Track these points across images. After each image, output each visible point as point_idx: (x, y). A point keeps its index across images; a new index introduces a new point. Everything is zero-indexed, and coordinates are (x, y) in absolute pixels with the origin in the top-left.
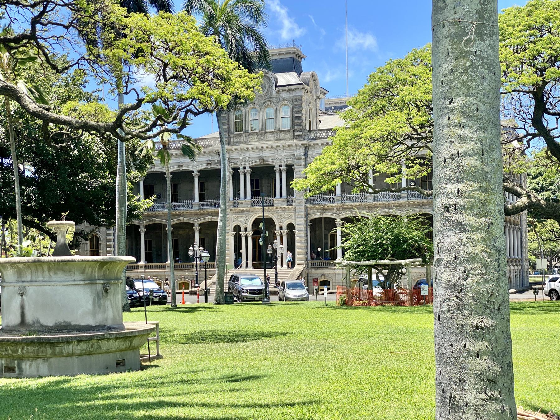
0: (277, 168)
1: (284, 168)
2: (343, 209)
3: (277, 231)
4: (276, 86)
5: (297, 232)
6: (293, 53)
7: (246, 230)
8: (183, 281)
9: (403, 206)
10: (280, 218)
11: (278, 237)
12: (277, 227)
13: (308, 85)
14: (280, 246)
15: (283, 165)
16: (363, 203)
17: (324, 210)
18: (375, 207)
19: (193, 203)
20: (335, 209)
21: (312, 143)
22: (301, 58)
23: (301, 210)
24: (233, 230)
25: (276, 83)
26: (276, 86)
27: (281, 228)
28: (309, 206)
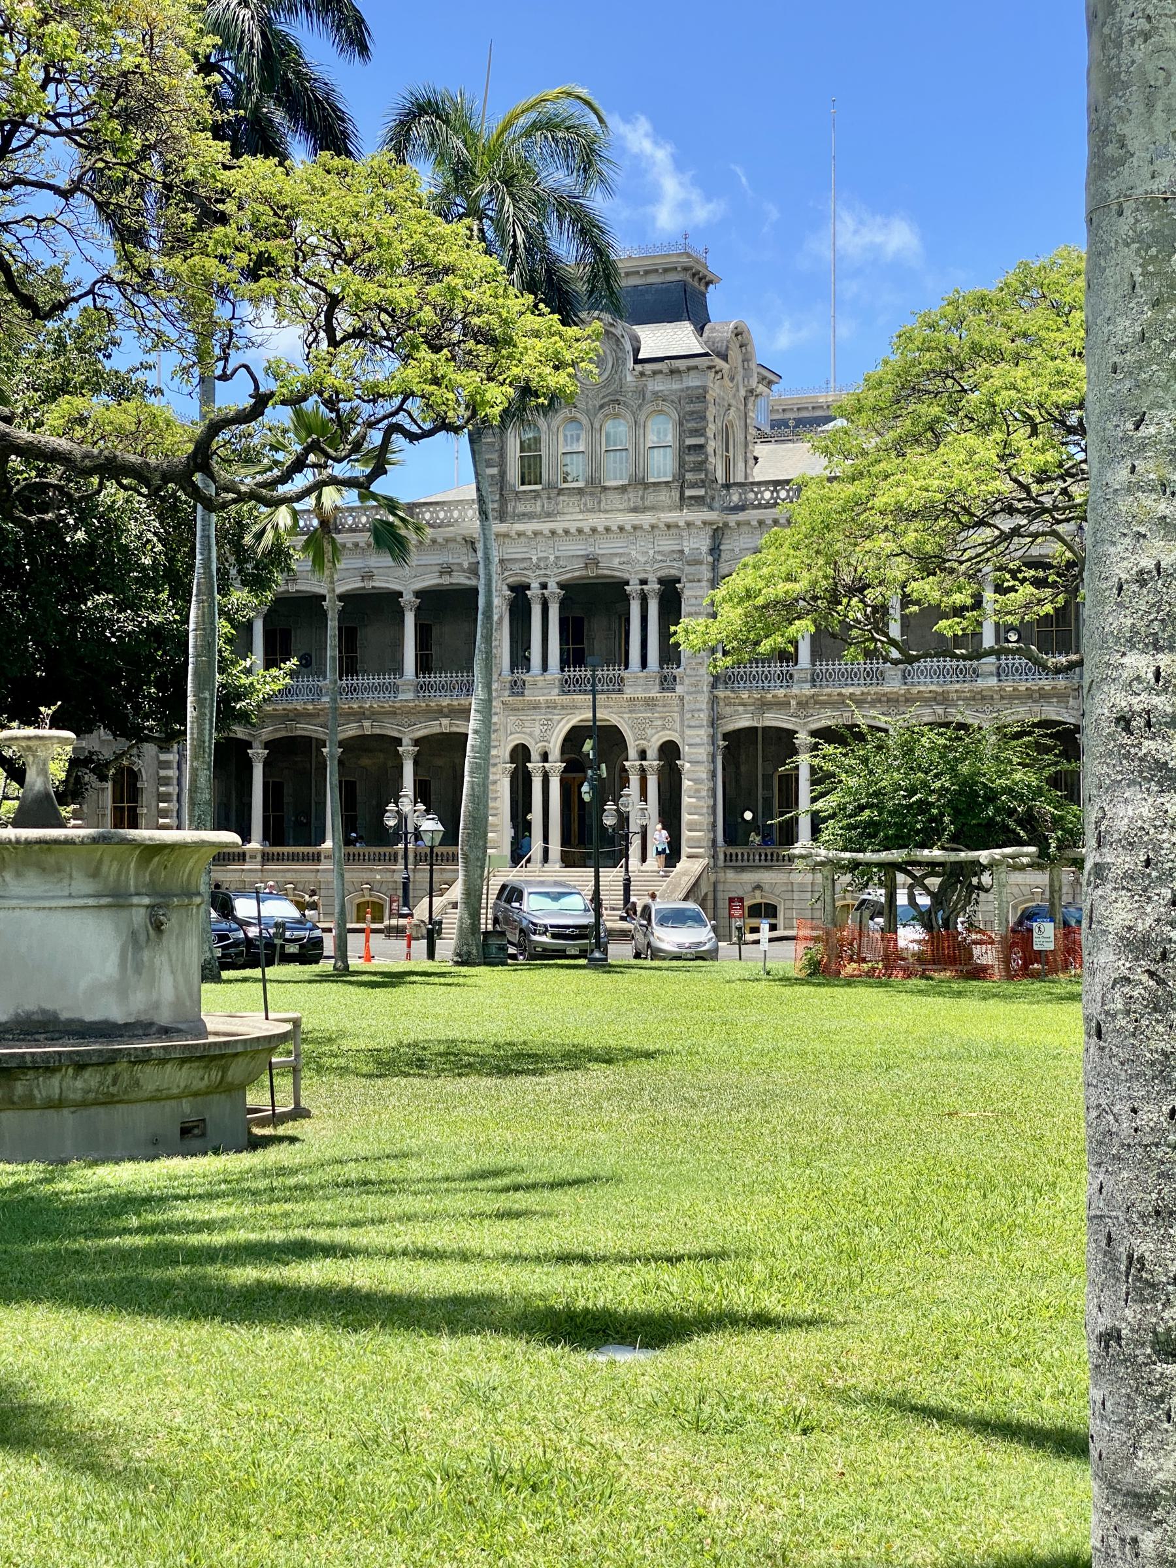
0: (633, 588)
1: (653, 586)
2: (816, 703)
3: (633, 763)
4: (637, 361)
5: (687, 765)
6: (686, 269)
7: (545, 757)
8: (367, 898)
9: (983, 698)
10: (641, 727)
11: (634, 780)
12: (632, 753)
13: (724, 357)
14: (639, 807)
15: (652, 578)
16: (873, 689)
17: (763, 706)
18: (907, 700)
19: (398, 682)
20: (793, 702)
21: (732, 519)
22: (707, 284)
23: (698, 706)
24: (507, 758)
25: (637, 351)
26: (637, 361)
27: (643, 755)
28: (721, 694)
